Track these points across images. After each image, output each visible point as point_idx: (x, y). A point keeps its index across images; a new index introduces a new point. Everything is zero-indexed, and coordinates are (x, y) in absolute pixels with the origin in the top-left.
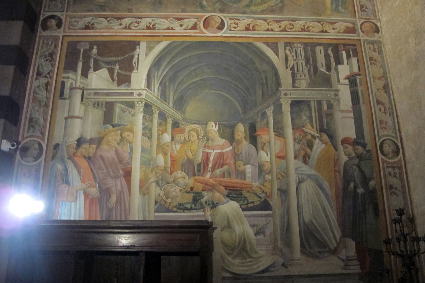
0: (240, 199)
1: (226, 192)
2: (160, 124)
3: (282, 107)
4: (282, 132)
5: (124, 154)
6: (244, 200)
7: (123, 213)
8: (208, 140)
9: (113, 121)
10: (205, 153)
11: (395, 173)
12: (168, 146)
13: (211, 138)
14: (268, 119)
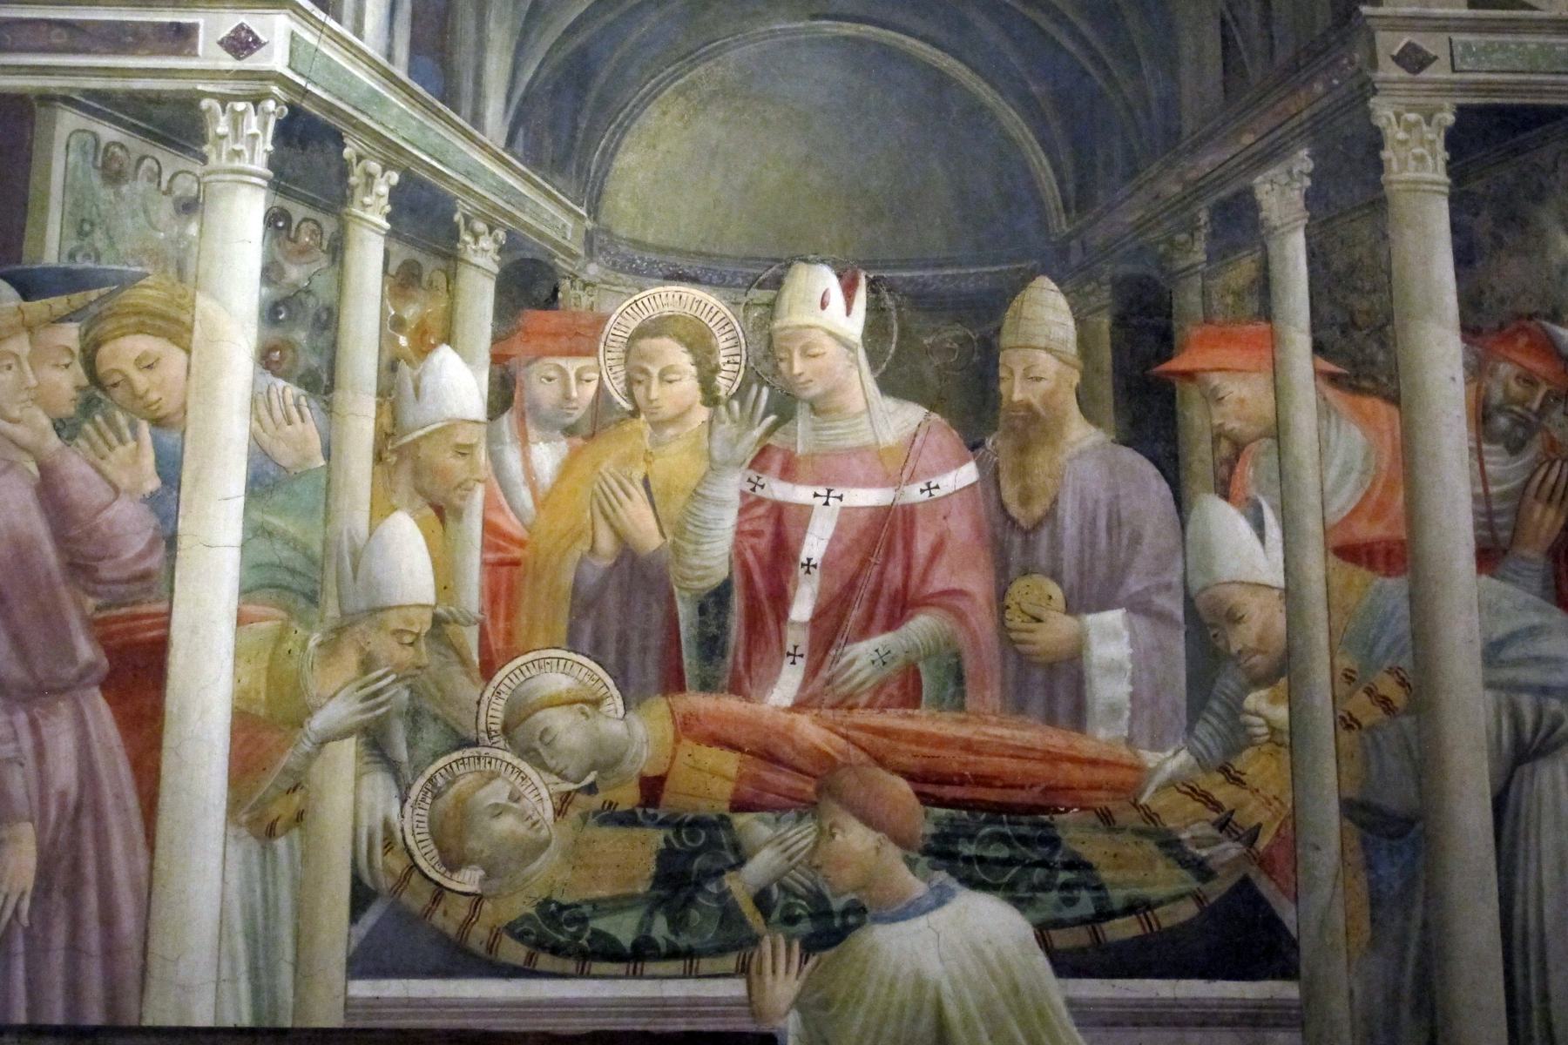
0: (1038, 874)
1: (924, 823)
2: (403, 280)
3: (1386, 154)
4: (1381, 357)
5: (107, 506)
6: (1066, 886)
7: (93, 972)
8: (785, 407)
9: (28, 246)
10: (761, 511)
12: (464, 451)
13: (815, 390)
14: (1265, 248)
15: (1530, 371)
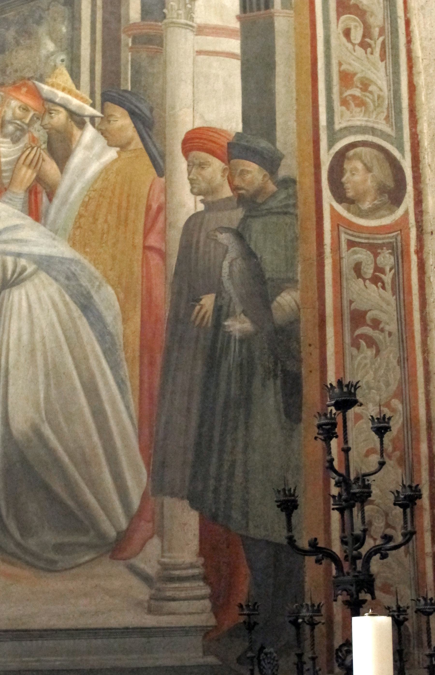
11: (379, 269)
15: (26, 105)
